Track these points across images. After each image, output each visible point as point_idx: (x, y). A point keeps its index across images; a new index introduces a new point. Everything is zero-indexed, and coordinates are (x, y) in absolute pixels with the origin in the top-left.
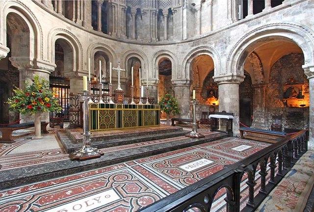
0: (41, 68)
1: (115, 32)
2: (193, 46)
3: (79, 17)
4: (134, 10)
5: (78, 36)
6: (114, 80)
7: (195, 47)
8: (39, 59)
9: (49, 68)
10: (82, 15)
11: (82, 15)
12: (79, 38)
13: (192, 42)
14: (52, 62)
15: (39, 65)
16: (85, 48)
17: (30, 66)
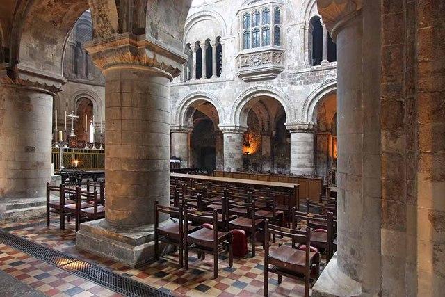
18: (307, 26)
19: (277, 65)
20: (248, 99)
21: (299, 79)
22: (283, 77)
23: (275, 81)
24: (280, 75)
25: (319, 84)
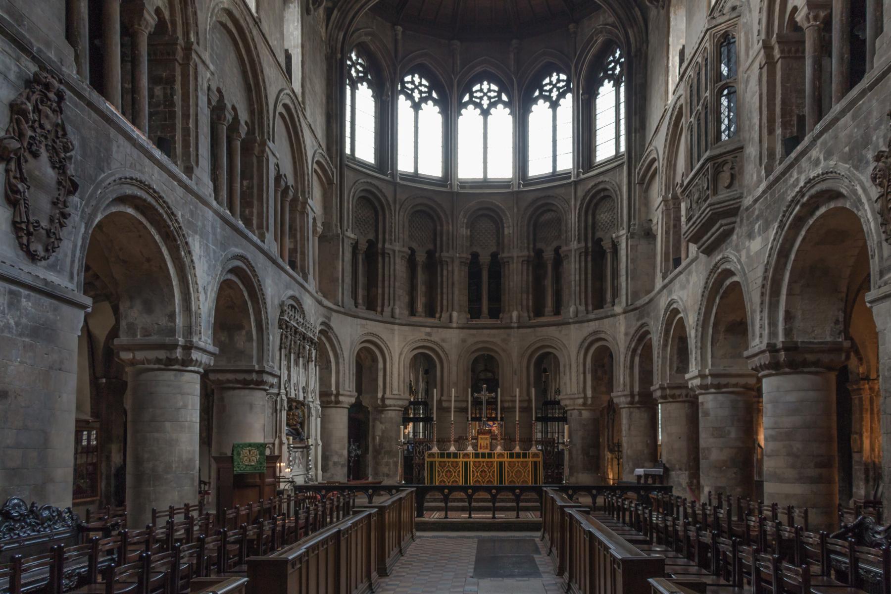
0: (390, 406)
1: (509, 311)
2: (638, 320)
3: (445, 308)
4: (549, 254)
5: (443, 340)
6: (506, 405)
7: (639, 323)
8: (388, 395)
9: (400, 403)
10: (450, 303)
11: (450, 303)
12: (444, 344)
13: (637, 311)
14: (404, 393)
15: (388, 402)
16: (453, 357)
17: (379, 406)
18: (777, 53)
19: (723, 195)
20: (717, 300)
21: (758, 218)
22: (742, 221)
23: (734, 237)
24: (738, 220)
25: (776, 225)
